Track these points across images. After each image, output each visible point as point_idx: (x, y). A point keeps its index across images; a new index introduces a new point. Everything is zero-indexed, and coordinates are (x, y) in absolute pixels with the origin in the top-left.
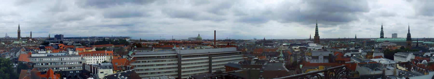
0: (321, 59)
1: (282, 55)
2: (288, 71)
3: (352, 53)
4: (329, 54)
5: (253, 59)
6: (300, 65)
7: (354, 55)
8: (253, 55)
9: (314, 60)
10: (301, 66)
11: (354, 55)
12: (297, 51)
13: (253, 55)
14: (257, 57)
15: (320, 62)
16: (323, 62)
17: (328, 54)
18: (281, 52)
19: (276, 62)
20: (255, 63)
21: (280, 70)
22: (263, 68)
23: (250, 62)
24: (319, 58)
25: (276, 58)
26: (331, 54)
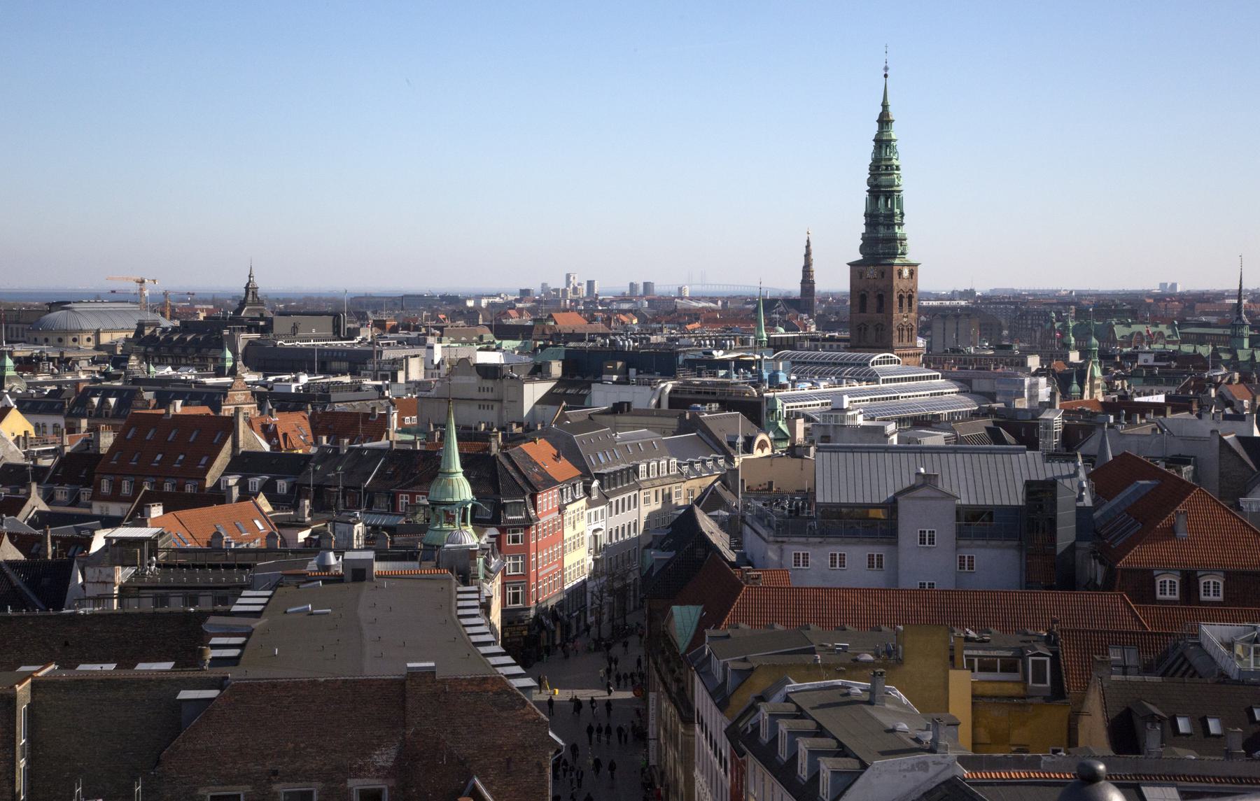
0: (926, 538)
2: (517, 683)
4: (1032, 488)
5: (98, 543)
6: (676, 609)
8: (105, 487)
9: (838, 550)
13: (105, 487)
14: (156, 511)
15: (908, 582)
16: (945, 582)
17: (1020, 488)
19: (378, 567)
21: (431, 672)
22: (220, 647)
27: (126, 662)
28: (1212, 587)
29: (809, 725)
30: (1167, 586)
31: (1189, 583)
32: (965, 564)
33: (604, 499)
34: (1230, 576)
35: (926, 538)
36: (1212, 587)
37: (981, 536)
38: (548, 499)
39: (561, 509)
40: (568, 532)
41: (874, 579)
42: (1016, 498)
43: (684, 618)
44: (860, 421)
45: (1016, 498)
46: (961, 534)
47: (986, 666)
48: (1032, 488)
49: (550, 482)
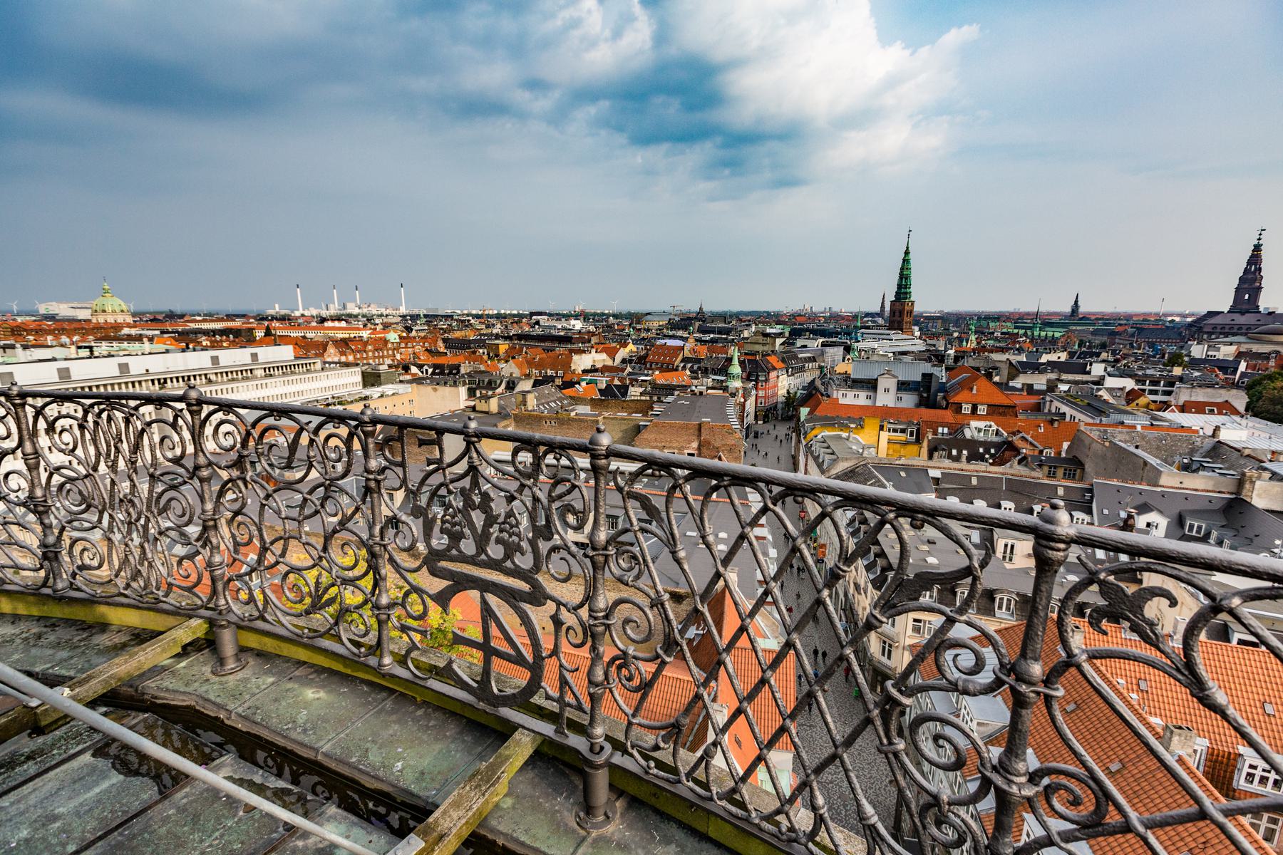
1: (736, 369)
3: (1053, 376)
4: (924, 375)
7: (1064, 387)
10: (804, 411)
11: (1064, 387)
12: (809, 358)
15: (879, 404)
16: (891, 404)
18: (736, 361)
19: (709, 391)
20: (642, 394)
23: (624, 389)
24: (882, 384)
25: (723, 378)
26: (931, 375)
27: (630, 414)
28: (982, 410)
29: (825, 445)
30: (966, 409)
31: (974, 408)
32: (900, 399)
33: (792, 375)
34: (989, 406)
35: (887, 390)
36: (982, 410)
37: (905, 390)
38: (773, 374)
39: (778, 377)
40: (780, 384)
41: (868, 403)
42: (919, 379)
43: (804, 411)
44: (881, 353)
45: (919, 379)
46: (899, 389)
47: (895, 431)
48: (924, 375)
49: (774, 369)
